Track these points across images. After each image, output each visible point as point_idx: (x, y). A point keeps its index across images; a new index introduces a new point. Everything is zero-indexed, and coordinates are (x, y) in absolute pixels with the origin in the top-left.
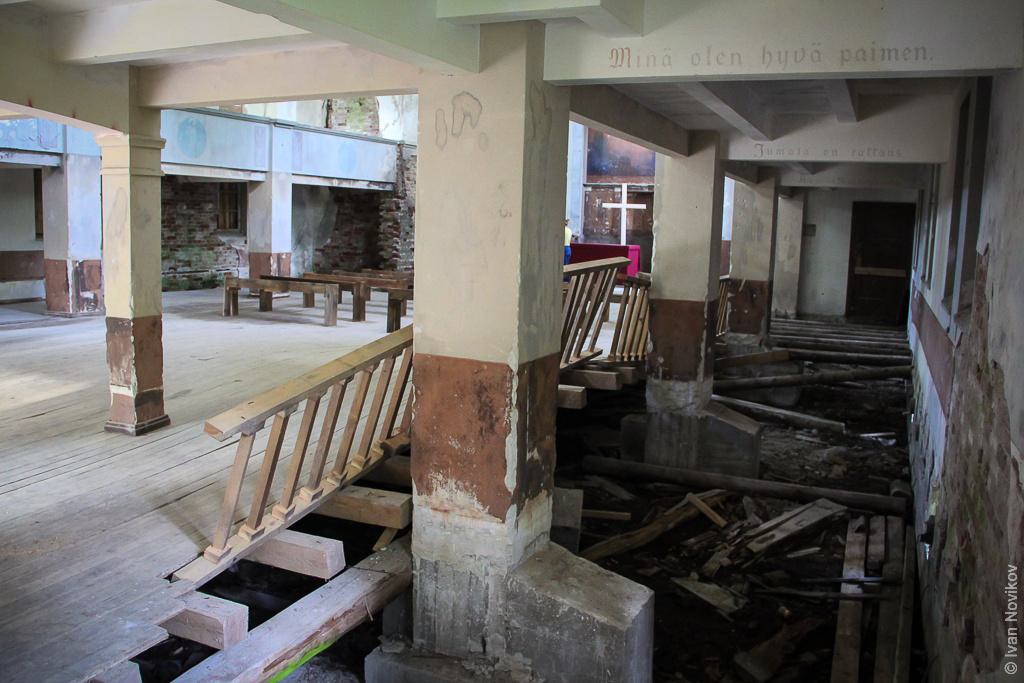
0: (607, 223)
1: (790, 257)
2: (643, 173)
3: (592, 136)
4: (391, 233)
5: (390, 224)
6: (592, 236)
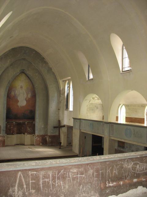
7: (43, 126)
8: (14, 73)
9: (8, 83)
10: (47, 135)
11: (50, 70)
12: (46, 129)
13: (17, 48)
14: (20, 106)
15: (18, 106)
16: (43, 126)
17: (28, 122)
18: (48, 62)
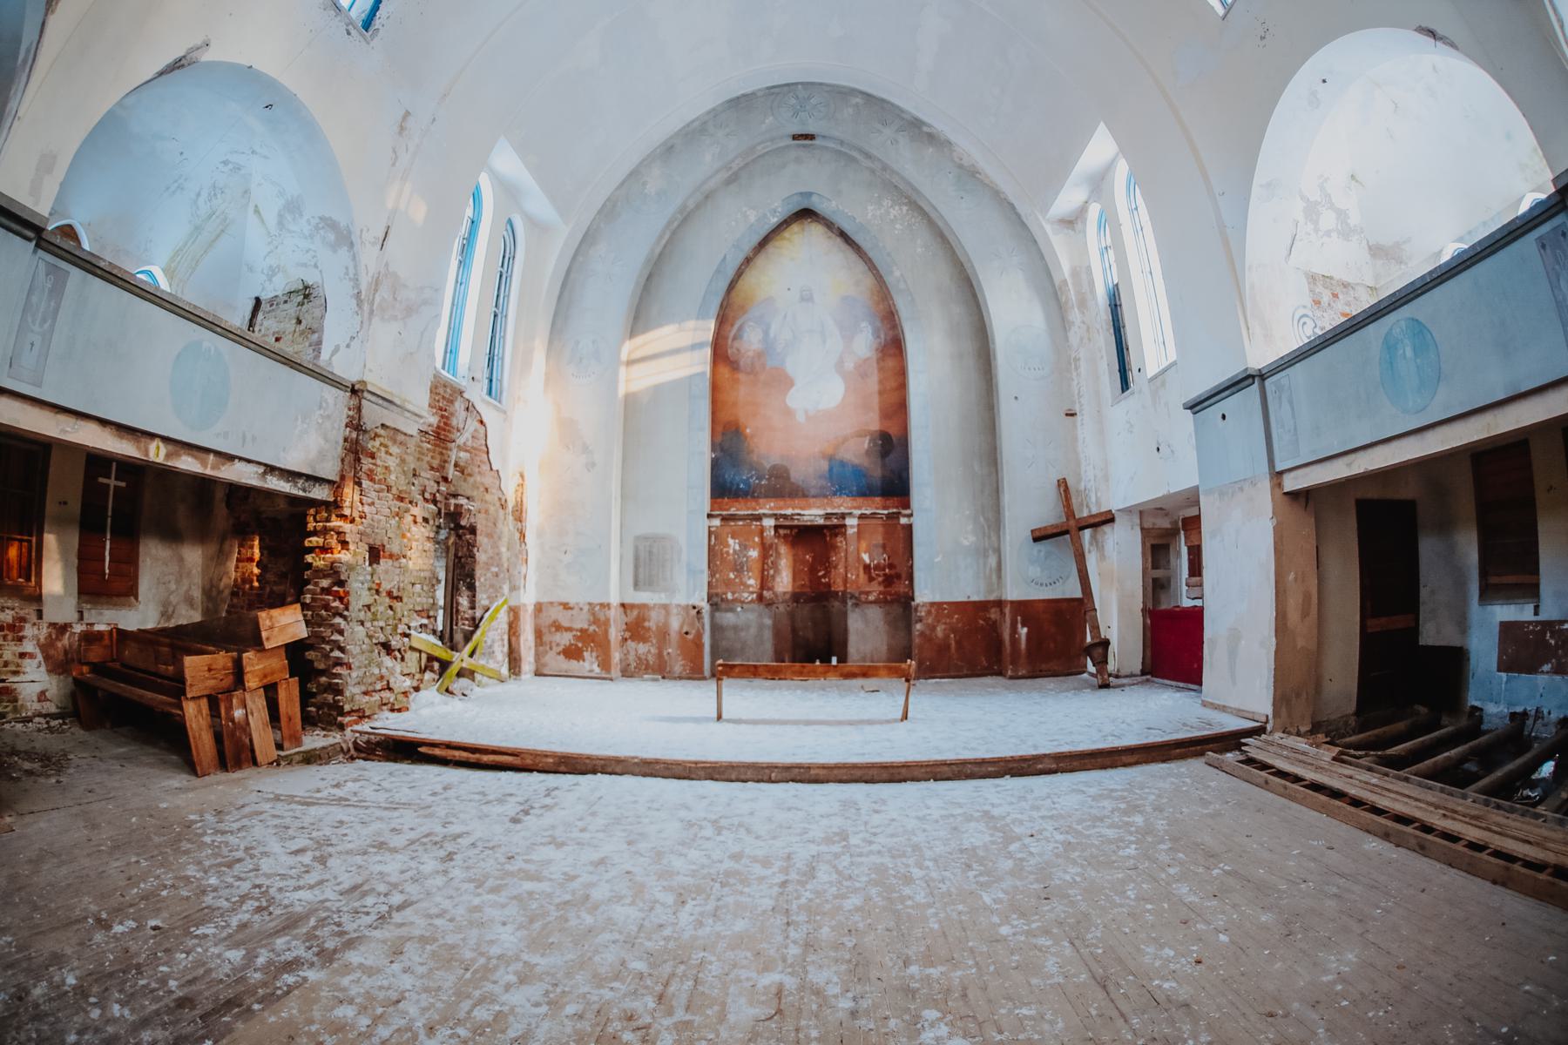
0: (751, 582)
1: (1305, 614)
2: (813, 492)
3: (719, 429)
4: (327, 607)
5: (325, 583)
6: (723, 606)
7: (969, 540)
8: (753, 217)
9: (718, 271)
10: (999, 604)
11: (969, 175)
12: (993, 561)
13: (753, 94)
14: (806, 412)
15: (788, 413)
16: (972, 539)
17: (861, 517)
18: (952, 138)
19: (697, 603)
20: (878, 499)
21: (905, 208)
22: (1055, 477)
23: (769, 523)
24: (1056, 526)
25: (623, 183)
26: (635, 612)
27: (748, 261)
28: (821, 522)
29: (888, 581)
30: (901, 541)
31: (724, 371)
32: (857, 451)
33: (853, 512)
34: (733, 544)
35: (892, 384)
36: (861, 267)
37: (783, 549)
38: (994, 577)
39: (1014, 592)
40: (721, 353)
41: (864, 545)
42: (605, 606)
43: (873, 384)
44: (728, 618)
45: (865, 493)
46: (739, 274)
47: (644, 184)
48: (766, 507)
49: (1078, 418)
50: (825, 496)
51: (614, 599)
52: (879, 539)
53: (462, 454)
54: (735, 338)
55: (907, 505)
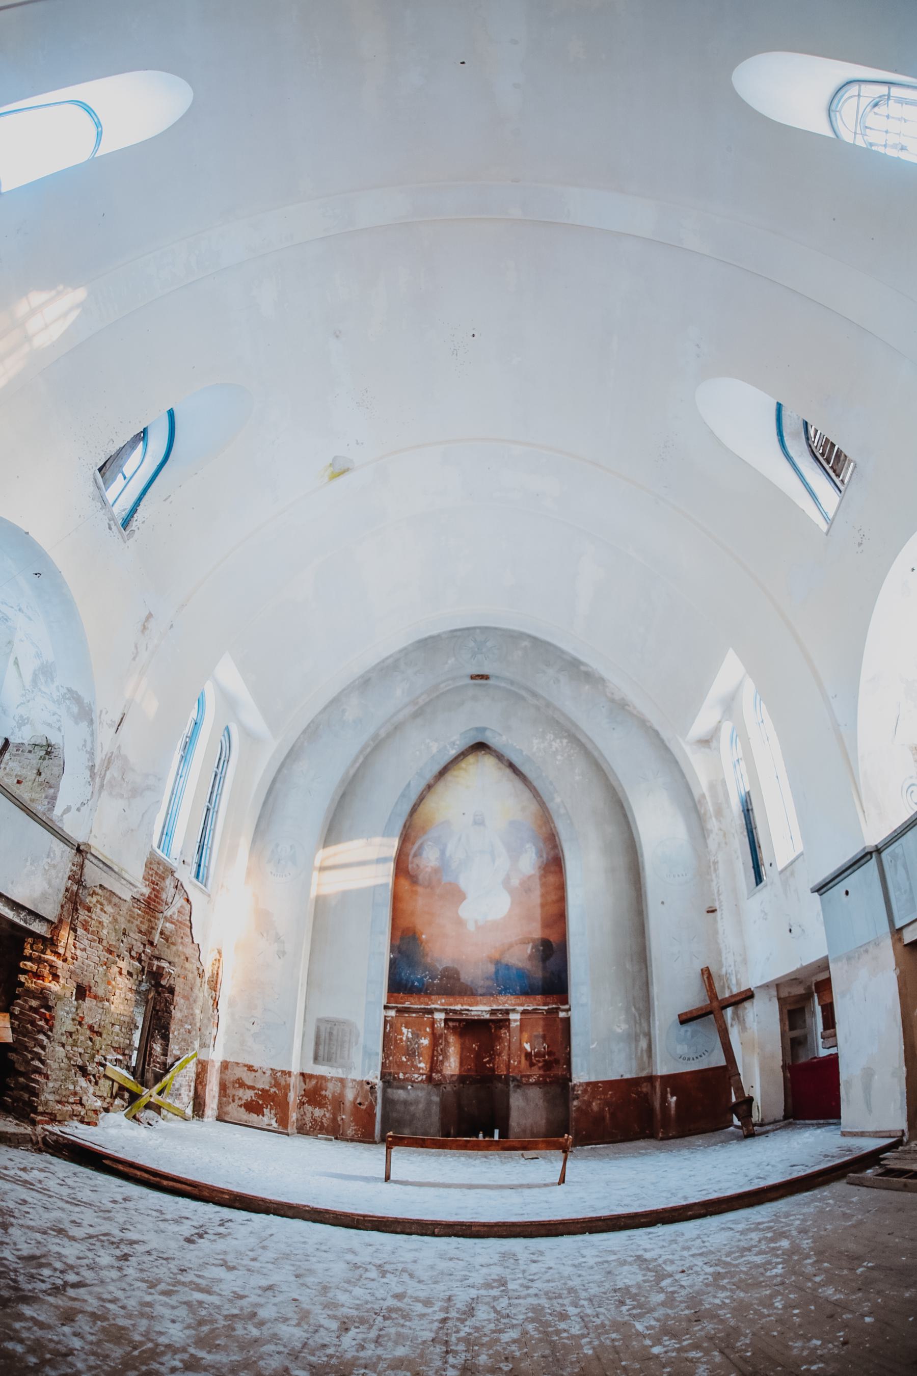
0: (422, 1065)
2: (480, 991)
3: (399, 934)
6: (395, 1083)
7: (621, 1028)
9: (403, 795)
11: (620, 708)
12: (643, 1044)
13: (439, 636)
14: (476, 922)
15: (460, 922)
16: (624, 1026)
17: (524, 1012)
19: (370, 1080)
20: (539, 997)
21: (565, 741)
22: (698, 966)
23: (440, 1016)
24: (701, 1009)
25: (325, 708)
26: (314, 1082)
27: (429, 787)
28: (487, 1016)
29: (548, 1066)
30: (559, 1033)
31: (405, 884)
32: (520, 956)
33: (517, 1010)
34: (406, 1033)
35: (553, 897)
36: (527, 794)
37: (452, 1039)
38: (645, 1058)
39: (662, 1068)
40: (403, 867)
41: (525, 1036)
42: (290, 1073)
43: (536, 897)
44: (400, 1094)
45: (528, 991)
46: (421, 799)
47: (344, 711)
48: (438, 1003)
49: (718, 913)
50: (492, 995)
51: (295, 1069)
52: (540, 1031)
53: (168, 925)
54: (415, 856)
55: (566, 1002)
